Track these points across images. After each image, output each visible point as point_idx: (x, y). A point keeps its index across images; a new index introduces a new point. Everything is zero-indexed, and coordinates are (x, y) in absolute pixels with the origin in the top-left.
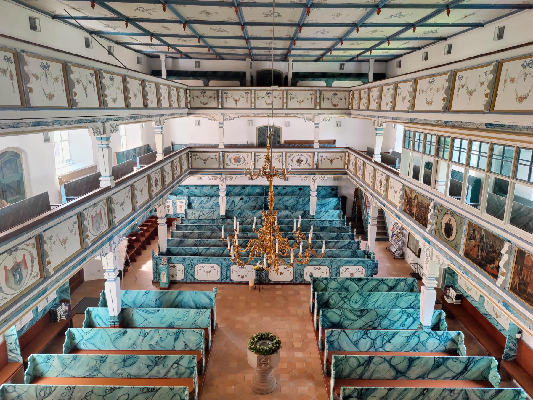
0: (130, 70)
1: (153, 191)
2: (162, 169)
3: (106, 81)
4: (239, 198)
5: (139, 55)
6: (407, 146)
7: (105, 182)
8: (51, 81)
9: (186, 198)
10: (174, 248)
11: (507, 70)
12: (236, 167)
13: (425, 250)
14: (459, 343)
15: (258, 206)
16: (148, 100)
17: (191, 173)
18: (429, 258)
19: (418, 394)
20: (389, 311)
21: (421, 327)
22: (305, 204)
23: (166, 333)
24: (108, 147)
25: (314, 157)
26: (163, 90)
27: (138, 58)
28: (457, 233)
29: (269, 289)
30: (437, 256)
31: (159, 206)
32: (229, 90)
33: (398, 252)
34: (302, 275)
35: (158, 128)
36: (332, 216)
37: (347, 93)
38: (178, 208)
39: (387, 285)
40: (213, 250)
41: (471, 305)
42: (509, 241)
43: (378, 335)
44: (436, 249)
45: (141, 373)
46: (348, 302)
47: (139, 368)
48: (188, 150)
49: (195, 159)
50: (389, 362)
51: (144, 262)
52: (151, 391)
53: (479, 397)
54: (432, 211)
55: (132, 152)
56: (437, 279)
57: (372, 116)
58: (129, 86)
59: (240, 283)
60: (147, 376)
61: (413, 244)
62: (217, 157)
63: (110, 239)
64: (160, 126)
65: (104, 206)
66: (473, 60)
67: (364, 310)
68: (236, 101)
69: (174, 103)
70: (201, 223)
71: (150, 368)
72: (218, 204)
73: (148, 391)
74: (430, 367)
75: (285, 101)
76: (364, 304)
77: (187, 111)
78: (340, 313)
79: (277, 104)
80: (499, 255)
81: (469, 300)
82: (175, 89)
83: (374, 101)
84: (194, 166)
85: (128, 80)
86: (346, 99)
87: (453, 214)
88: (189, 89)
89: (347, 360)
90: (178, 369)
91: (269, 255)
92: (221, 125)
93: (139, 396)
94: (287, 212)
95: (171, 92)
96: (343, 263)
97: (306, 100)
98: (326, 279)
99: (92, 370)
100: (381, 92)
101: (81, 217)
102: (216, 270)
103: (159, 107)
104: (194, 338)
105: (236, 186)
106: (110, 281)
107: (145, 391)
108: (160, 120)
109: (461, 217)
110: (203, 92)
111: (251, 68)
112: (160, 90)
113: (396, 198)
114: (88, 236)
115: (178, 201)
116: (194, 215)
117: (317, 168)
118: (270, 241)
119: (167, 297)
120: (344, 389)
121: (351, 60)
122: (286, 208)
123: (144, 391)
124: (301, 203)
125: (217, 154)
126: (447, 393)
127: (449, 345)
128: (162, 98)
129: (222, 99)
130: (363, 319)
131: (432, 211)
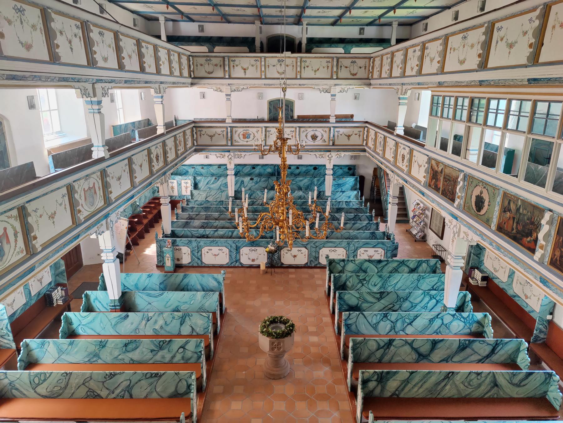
0: (122, 25)
1: (154, 166)
2: (164, 143)
3: (94, 35)
4: (249, 178)
5: (135, 16)
6: (434, 113)
7: (98, 152)
8: (28, 28)
9: (191, 178)
10: (179, 230)
11: (557, 13)
12: (245, 143)
13: (452, 227)
14: (485, 325)
15: (269, 187)
16: (145, 63)
17: (196, 151)
18: (456, 235)
19: (443, 377)
20: (410, 293)
21: (445, 308)
22: (320, 185)
23: (172, 316)
24: (99, 113)
25: (330, 133)
26: (163, 54)
27: (134, 19)
28: (489, 205)
29: (282, 273)
30: (465, 233)
31: (162, 184)
32: (237, 57)
33: (420, 234)
34: (317, 258)
35: (157, 97)
36: (349, 197)
37: (367, 60)
38: (183, 189)
39: (408, 267)
40: (221, 232)
41: (497, 287)
42: (551, 211)
43: (399, 318)
44: (464, 225)
45: (145, 358)
46: (366, 285)
47: (143, 353)
48: (193, 125)
49: (200, 135)
50: (411, 344)
51: (148, 246)
52: (155, 376)
53: (508, 381)
54: (461, 183)
55: (130, 125)
56: (463, 258)
57: (395, 84)
58: (121, 43)
59: (251, 267)
60: (151, 362)
61: (436, 225)
62: (225, 133)
63: (106, 216)
64: (160, 95)
65: (98, 179)
66: (516, 5)
67: (384, 292)
68: (245, 69)
69: (175, 70)
70: (209, 204)
71: (155, 352)
72: (226, 185)
73: (151, 377)
74: (455, 350)
75: (299, 69)
76: (383, 286)
77: (190, 80)
78: (357, 295)
79: (290, 73)
80: (538, 227)
81: (496, 281)
82: (176, 55)
83: (398, 67)
84: (199, 143)
85: (121, 37)
86: (365, 67)
87: (485, 184)
88: (192, 56)
89: (366, 343)
90: (184, 354)
91: (281, 230)
92: (229, 97)
93: (142, 382)
94: (301, 193)
95: (172, 57)
96: (361, 244)
97: (321, 68)
98: (343, 260)
99: (92, 356)
100: (406, 55)
101: (70, 190)
102: (225, 253)
103: (158, 72)
104: (202, 322)
105: (245, 165)
106: (108, 262)
107: (148, 376)
108: (159, 88)
109: (495, 188)
110: (208, 59)
111: (261, 32)
112: (159, 53)
113: (420, 173)
114: (80, 211)
115: (183, 181)
116: (200, 196)
117: (333, 145)
118: (283, 214)
119: (172, 279)
120: (363, 373)
121: (370, 24)
122: (300, 189)
123: (147, 376)
124: (316, 183)
125: (225, 129)
126: (474, 376)
127: (474, 328)
128: (161, 63)
129: (229, 68)
130: (382, 301)
131: (461, 183)
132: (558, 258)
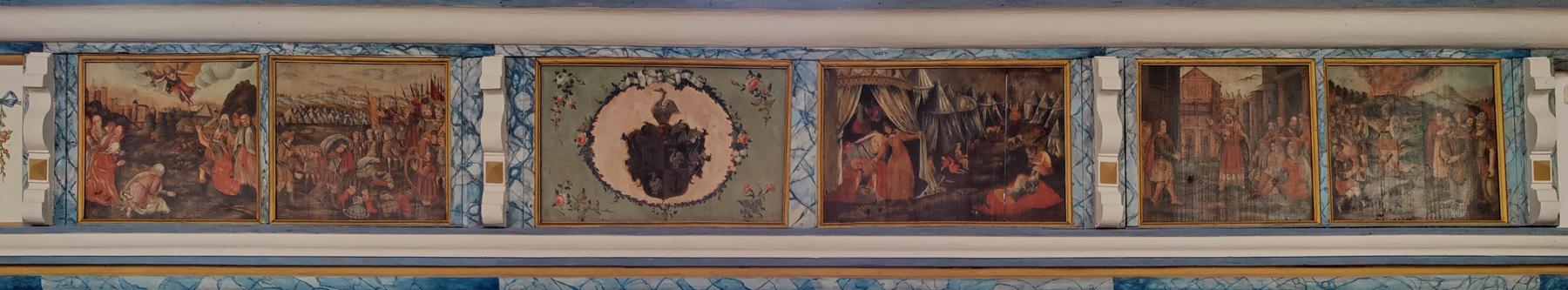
28: (737, 146)
132: (1170, 189)
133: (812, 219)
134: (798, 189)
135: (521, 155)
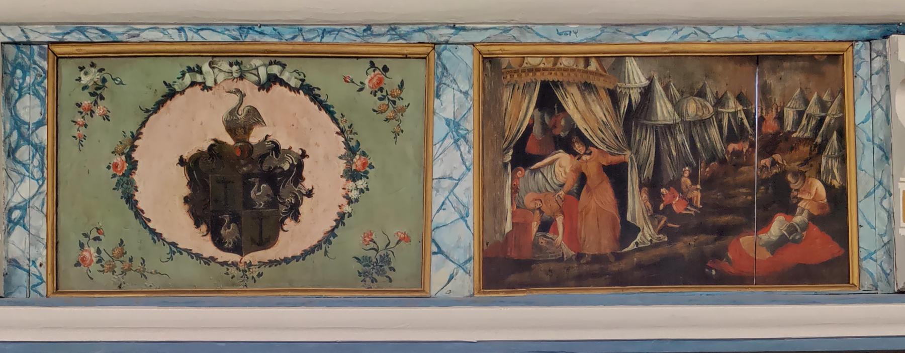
28: (352, 175)
133: (466, 283)
134: (445, 238)
135: (27, 188)
